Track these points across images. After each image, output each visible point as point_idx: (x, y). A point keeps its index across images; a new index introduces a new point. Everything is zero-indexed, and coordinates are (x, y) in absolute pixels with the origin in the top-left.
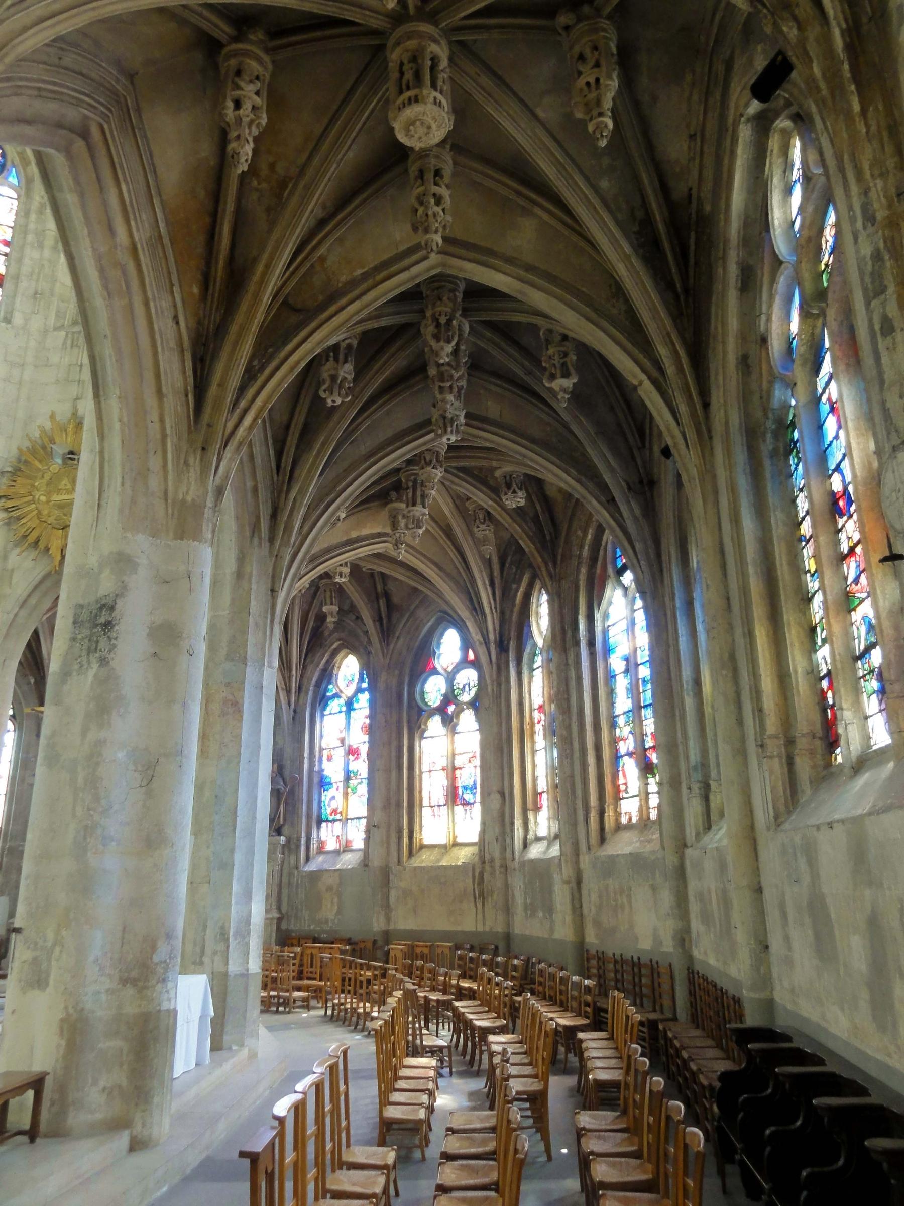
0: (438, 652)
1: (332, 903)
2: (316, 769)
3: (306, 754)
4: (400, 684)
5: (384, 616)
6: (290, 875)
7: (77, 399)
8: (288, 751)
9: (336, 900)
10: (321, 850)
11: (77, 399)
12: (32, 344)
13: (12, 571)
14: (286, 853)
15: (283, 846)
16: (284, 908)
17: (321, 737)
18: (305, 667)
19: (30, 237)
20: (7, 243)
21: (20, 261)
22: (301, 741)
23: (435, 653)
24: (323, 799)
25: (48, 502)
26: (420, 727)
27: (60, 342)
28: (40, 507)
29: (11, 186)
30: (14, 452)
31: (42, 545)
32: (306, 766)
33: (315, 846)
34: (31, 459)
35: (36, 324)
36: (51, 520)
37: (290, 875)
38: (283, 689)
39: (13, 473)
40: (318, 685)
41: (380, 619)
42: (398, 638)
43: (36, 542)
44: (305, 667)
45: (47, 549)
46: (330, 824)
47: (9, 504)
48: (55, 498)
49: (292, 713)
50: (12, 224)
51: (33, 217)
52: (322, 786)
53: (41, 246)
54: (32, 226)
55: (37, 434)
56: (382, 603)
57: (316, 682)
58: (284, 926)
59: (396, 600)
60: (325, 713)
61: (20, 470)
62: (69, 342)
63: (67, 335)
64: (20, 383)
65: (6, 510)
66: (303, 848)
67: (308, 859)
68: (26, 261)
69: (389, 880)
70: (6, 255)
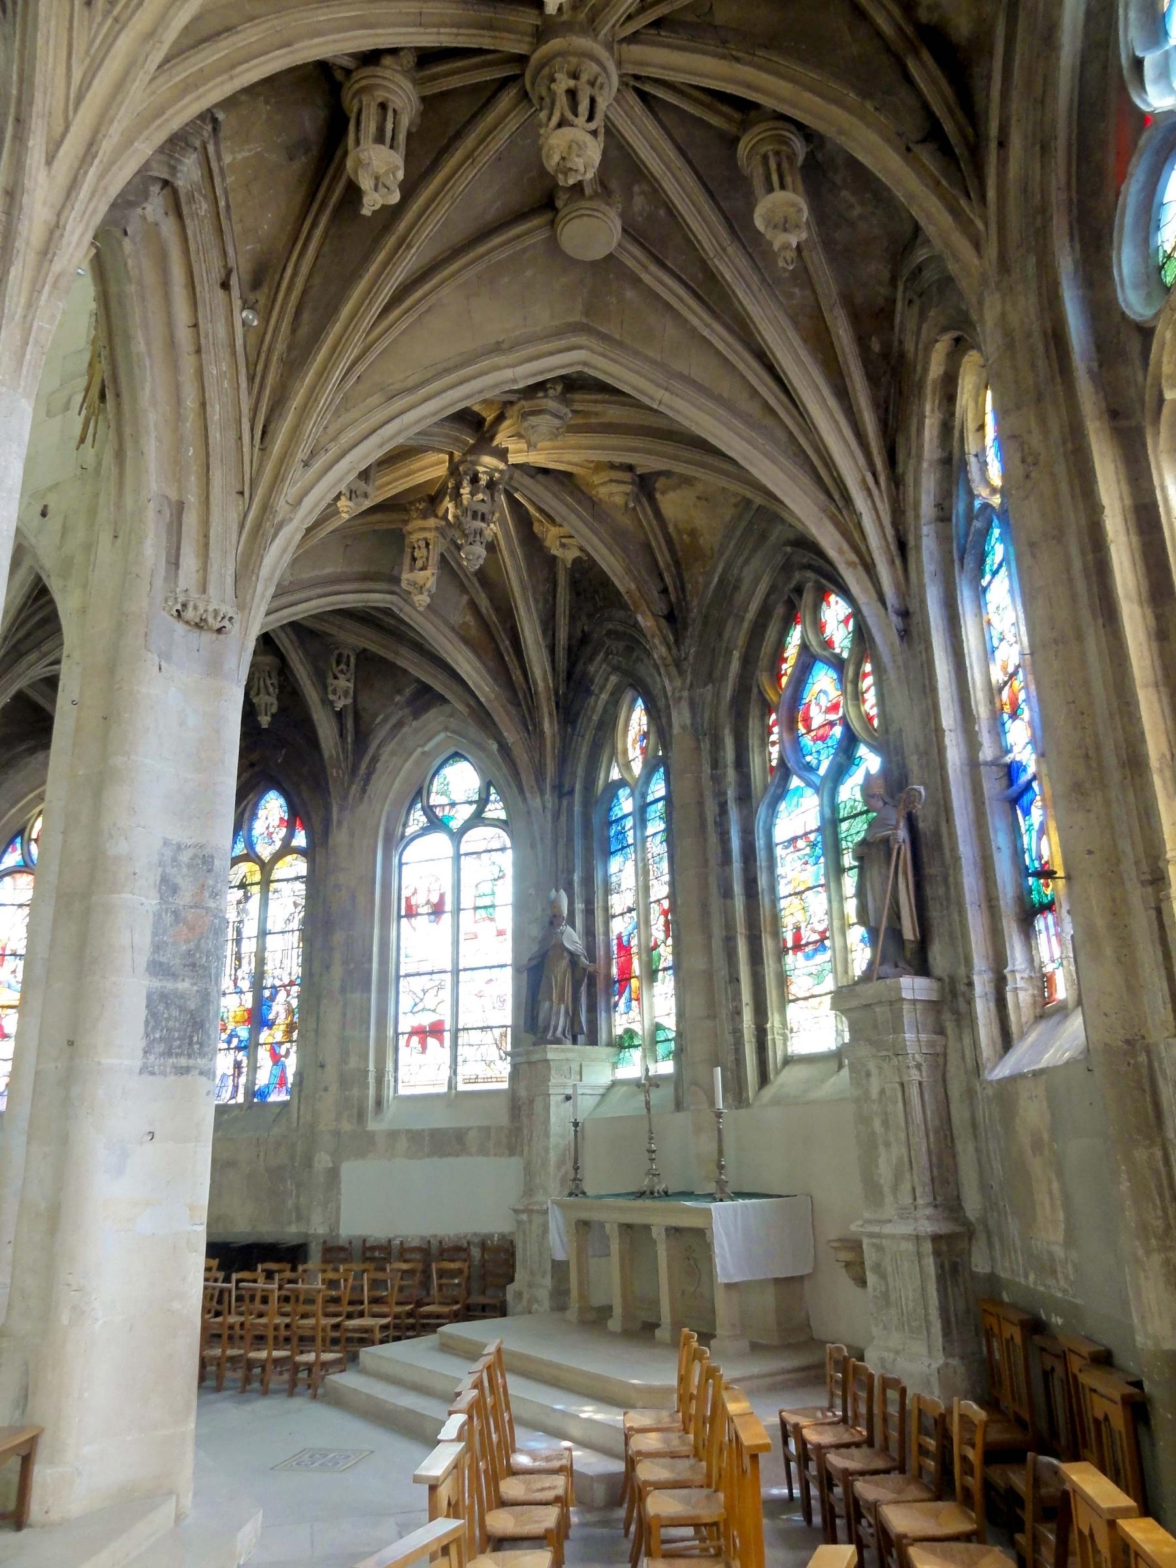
0: (1150, 60)
1: (1050, 1193)
2: (987, 753)
3: (948, 717)
4: (1051, 302)
5: (939, 110)
6: (970, 1093)
8: (912, 734)
9: (1055, 1186)
10: (1047, 1011)
14: (950, 1027)
15: (934, 1007)
16: (972, 1205)
17: (988, 654)
18: (896, 481)
22: (929, 688)
23: (1138, 64)
24: (1026, 839)
26: (1161, 400)
32: (954, 754)
33: (1025, 997)
37: (970, 1093)
38: (850, 564)
40: (944, 516)
41: (934, 134)
42: (1002, 144)
44: (896, 481)
46: (1050, 917)
49: (895, 620)
52: (1015, 801)
56: (925, 73)
57: (940, 506)
58: (980, 1264)
59: (962, 26)
60: (984, 583)
66: (983, 1009)
67: (1006, 1041)
69: (1157, 1105)
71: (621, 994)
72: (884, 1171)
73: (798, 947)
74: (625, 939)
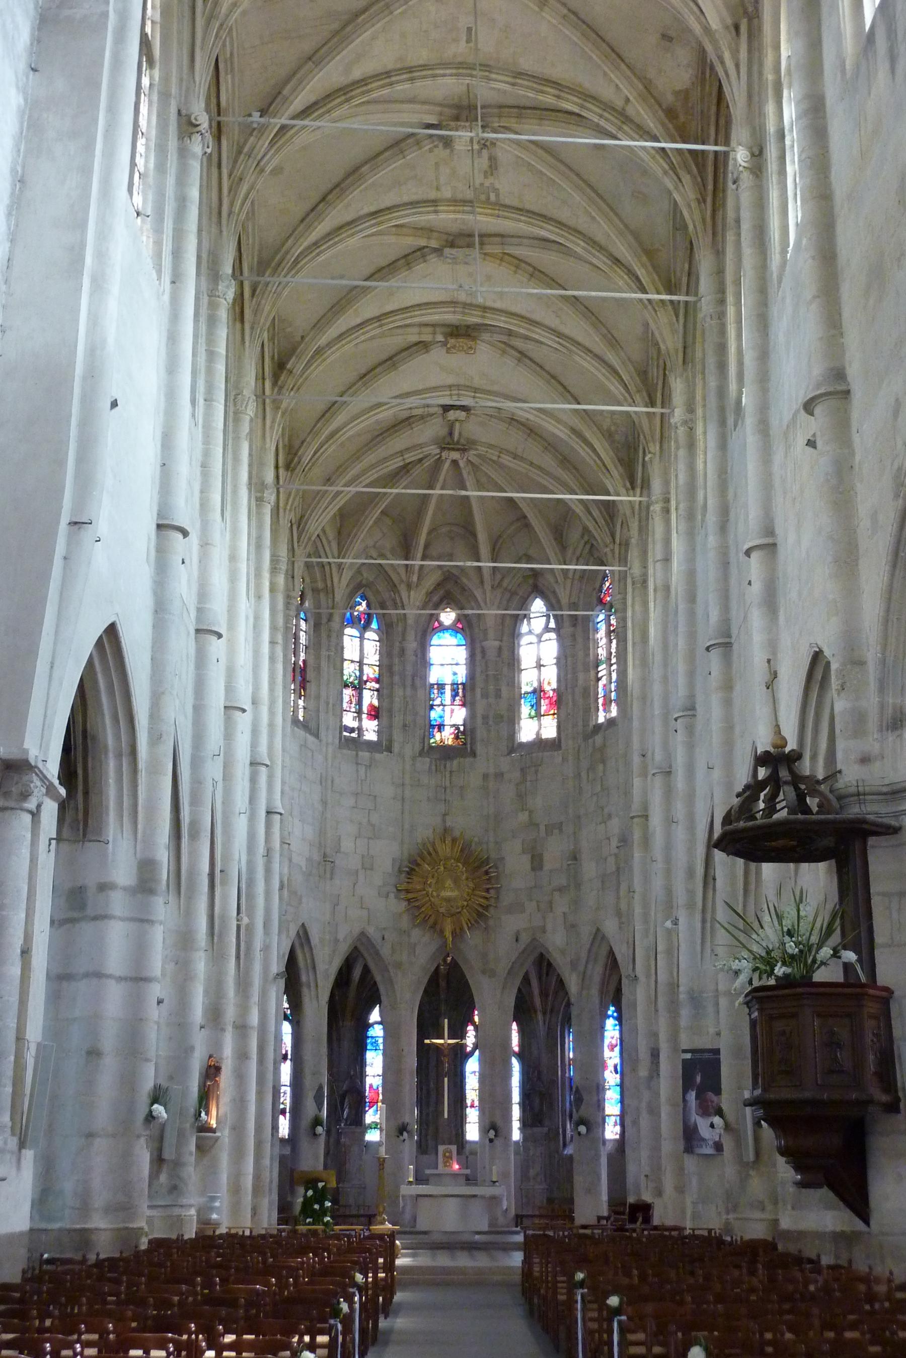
7: (445, 815)
11: (445, 815)
12: (408, 767)
13: (415, 944)
19: (396, 678)
20: (377, 681)
21: (391, 696)
25: (438, 896)
27: (427, 766)
28: (432, 899)
29: (375, 631)
30: (406, 854)
31: (438, 927)
34: (419, 860)
35: (408, 751)
36: (442, 910)
39: (408, 873)
43: (433, 927)
45: (442, 932)
47: (410, 896)
48: (444, 894)
50: (378, 663)
51: (396, 660)
53: (404, 686)
54: (396, 668)
55: (419, 841)
61: (414, 870)
62: (434, 767)
63: (431, 762)
64: (403, 799)
65: (409, 900)
66: (561, 1136)
67: (565, 1145)
68: (397, 699)
70: (377, 690)
71: (370, 1107)
72: (532, 1173)
73: (472, 1106)
74: (375, 1087)
